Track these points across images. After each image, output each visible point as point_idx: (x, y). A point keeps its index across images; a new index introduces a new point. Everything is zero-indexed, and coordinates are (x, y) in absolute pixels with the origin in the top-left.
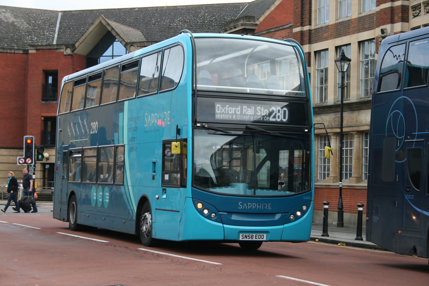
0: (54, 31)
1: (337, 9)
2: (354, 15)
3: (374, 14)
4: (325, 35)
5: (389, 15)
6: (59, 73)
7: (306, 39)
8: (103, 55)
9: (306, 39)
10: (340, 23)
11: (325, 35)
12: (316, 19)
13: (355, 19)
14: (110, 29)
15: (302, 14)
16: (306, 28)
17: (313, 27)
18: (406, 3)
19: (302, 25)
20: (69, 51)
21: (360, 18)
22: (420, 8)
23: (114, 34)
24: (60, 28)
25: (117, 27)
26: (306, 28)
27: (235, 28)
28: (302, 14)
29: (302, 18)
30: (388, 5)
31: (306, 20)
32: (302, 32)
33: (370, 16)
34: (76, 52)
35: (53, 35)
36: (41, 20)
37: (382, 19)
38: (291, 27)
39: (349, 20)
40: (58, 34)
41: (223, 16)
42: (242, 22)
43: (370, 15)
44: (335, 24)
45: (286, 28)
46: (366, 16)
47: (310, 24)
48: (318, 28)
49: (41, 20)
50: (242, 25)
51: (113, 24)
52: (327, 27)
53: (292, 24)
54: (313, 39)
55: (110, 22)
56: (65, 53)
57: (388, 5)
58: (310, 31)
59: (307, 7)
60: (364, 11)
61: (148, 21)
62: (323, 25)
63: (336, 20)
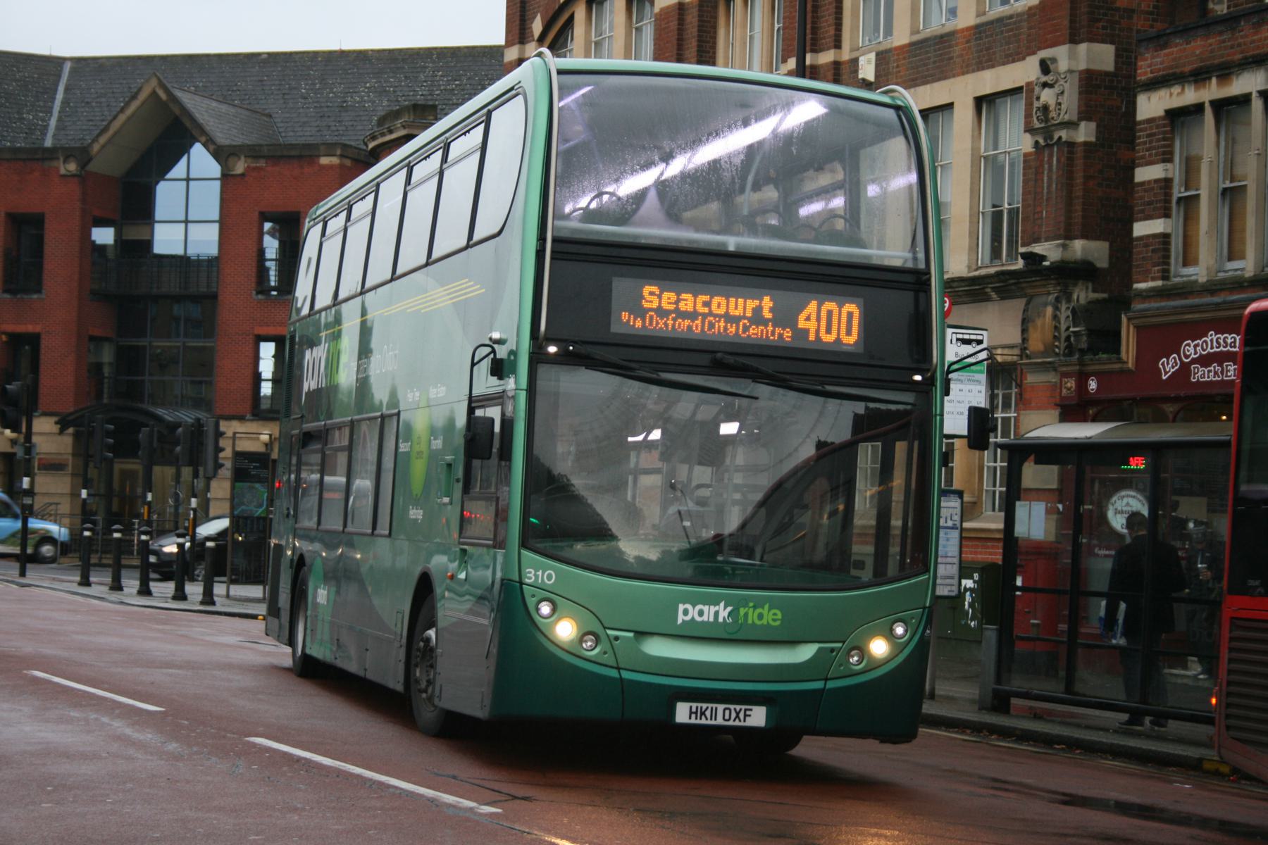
0: (49, 111)
6: (47, 221)
8: (169, 176)
14: (177, 111)
20: (72, 167)
23: (188, 124)
24: (65, 102)
25: (200, 107)
27: (391, 132)
34: (91, 167)
35: (46, 121)
36: (16, 80)
40: (60, 119)
49: (16, 80)
50: (404, 127)
51: (187, 99)
55: (178, 94)
56: (63, 171)
61: (290, 89)
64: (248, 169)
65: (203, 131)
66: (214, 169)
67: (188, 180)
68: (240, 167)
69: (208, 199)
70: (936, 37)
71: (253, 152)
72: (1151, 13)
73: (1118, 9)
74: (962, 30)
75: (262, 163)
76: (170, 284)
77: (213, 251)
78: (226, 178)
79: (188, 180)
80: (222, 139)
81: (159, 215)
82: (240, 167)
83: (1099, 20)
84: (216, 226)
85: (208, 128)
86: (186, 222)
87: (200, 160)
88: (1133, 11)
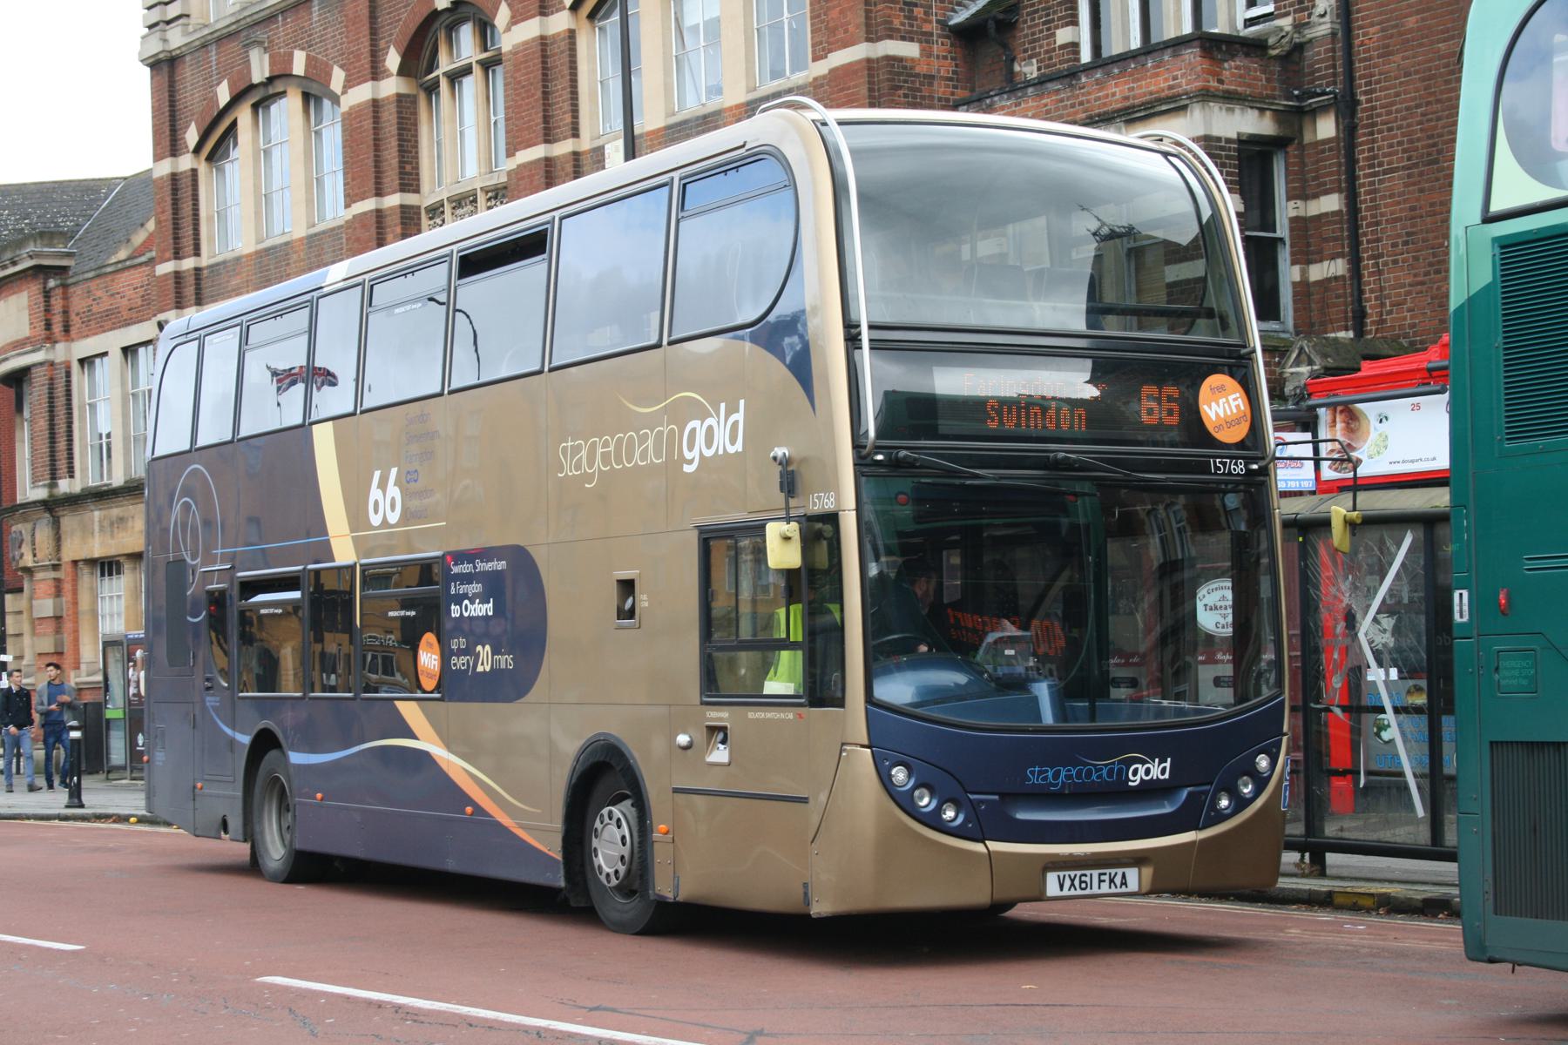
1: (257, 213)
2: (300, 232)
3: (341, 227)
4: (235, 282)
5: (373, 230)
7: (190, 291)
9: (190, 291)
10: (267, 250)
11: (235, 282)
12: (211, 239)
13: (301, 240)
15: (176, 227)
16: (188, 264)
17: (204, 261)
18: (411, 199)
19: (177, 256)
21: (310, 237)
22: (475, 201)
26: (188, 264)
27: (14, 263)
28: (176, 227)
29: (176, 238)
30: (369, 205)
31: (187, 242)
32: (178, 276)
33: (333, 232)
37: (358, 240)
38: (151, 262)
39: (287, 244)
41: (54, 216)
42: (31, 248)
43: (333, 229)
44: (257, 252)
45: (140, 264)
46: (324, 232)
47: (197, 253)
48: (218, 264)
50: (31, 257)
52: (238, 259)
53: (153, 254)
54: (206, 292)
57: (369, 205)
58: (198, 270)
59: (186, 209)
60: (322, 219)
62: (228, 256)
63: (259, 241)
70: (697, 118)
72: (951, 79)
73: (917, 75)
74: (731, 109)
83: (900, 88)
88: (932, 77)
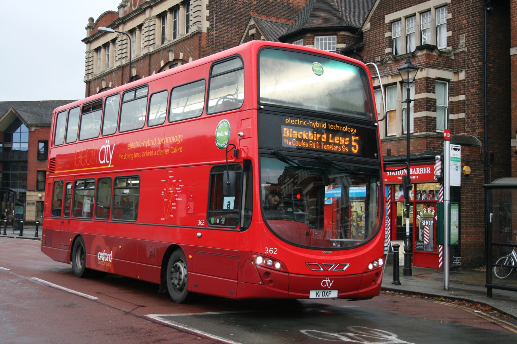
64: (35, 130)
65: (24, 121)
66: (27, 130)
67: (21, 132)
68: (33, 129)
69: (25, 137)
71: (36, 126)
75: (39, 128)
76: (16, 158)
77: (27, 149)
78: (29, 132)
79: (21, 132)
80: (29, 122)
81: (14, 141)
82: (33, 129)
84: (27, 144)
85: (25, 120)
86: (20, 143)
87: (24, 127)
